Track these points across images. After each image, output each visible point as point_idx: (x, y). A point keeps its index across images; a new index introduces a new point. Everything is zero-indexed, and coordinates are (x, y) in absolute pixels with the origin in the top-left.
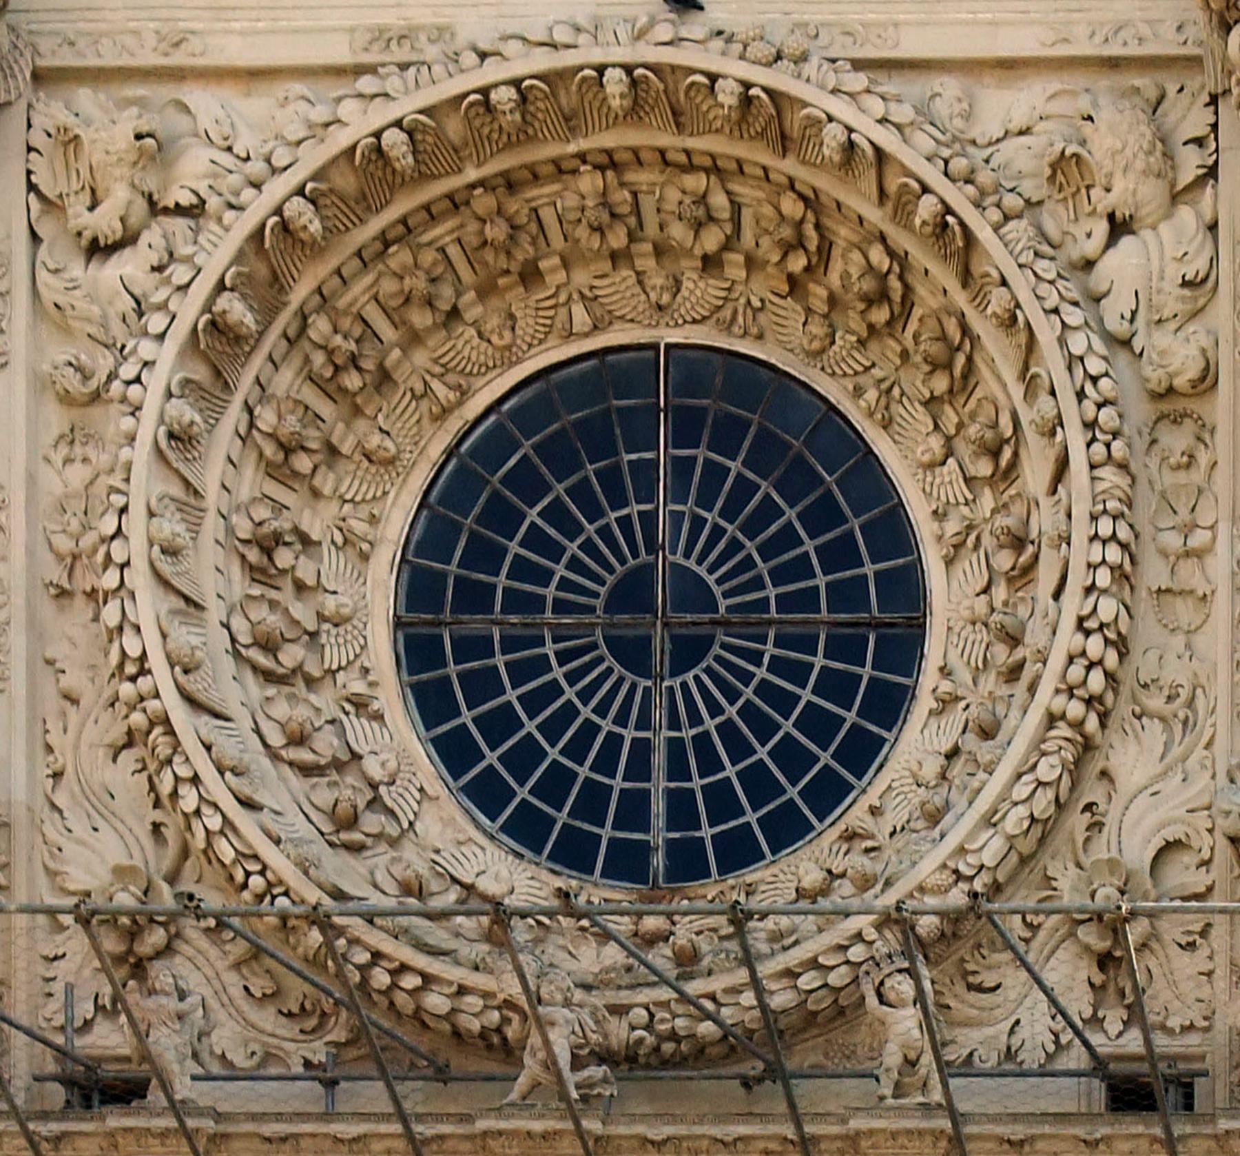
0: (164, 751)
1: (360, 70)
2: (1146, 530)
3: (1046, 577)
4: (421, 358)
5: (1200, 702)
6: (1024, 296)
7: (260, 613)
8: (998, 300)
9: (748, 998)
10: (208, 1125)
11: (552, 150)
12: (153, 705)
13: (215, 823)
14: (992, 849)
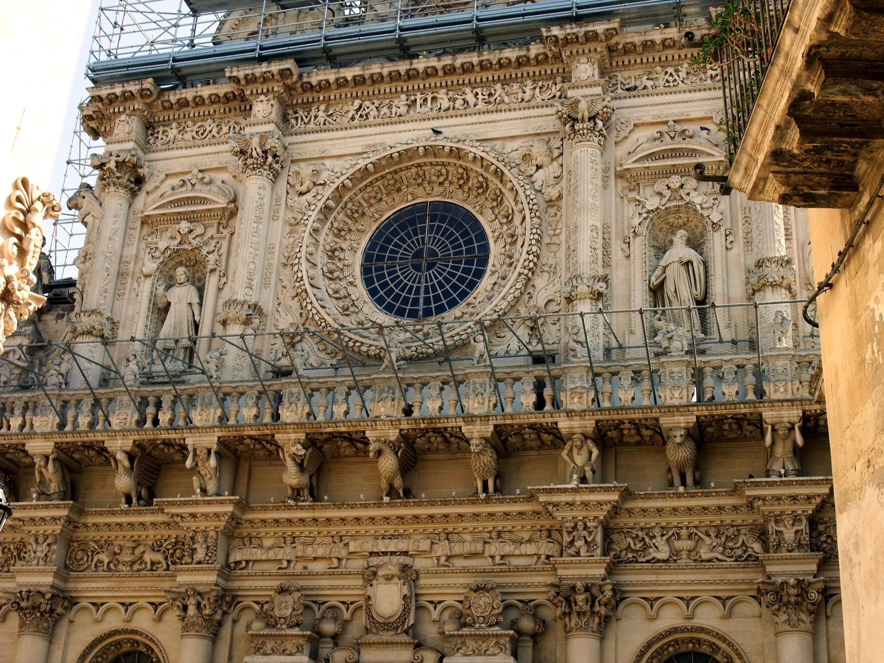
0: (304, 297)
1: (363, 153)
2: (544, 231)
3: (519, 243)
4: (372, 209)
5: (558, 268)
6: (515, 183)
7: (330, 266)
8: (509, 185)
9: (441, 343)
10: (306, 380)
11: (406, 164)
12: (303, 287)
13: (314, 311)
14: (504, 304)
